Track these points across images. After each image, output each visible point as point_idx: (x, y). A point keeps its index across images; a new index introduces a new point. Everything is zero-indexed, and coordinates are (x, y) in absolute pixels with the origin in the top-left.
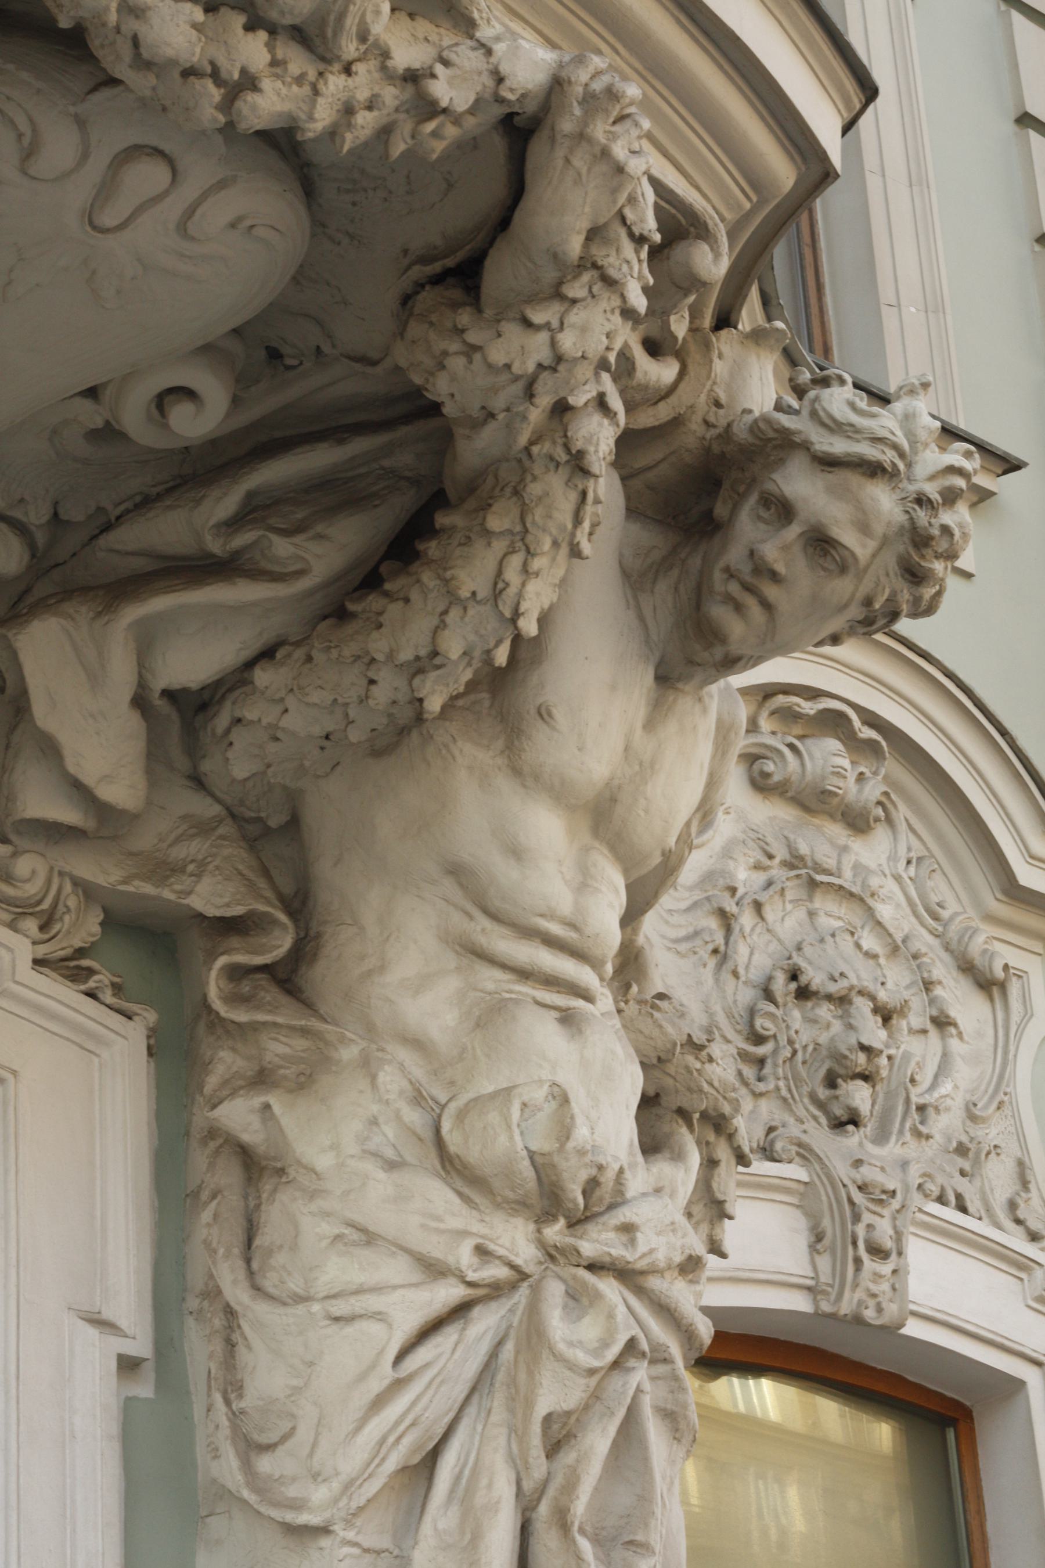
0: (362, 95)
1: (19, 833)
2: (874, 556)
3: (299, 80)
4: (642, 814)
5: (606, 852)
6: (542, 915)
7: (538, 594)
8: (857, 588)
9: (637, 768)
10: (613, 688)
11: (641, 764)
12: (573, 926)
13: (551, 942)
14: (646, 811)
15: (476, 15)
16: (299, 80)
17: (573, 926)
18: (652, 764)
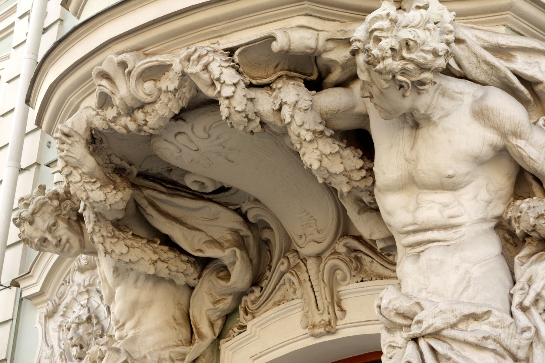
0: (166, 101)
1: (392, 251)
2: (370, 75)
3: (153, 111)
4: (423, 175)
5: (427, 191)
6: (404, 227)
7: (309, 158)
8: (377, 87)
9: (414, 163)
10: (391, 147)
11: (414, 161)
12: (415, 224)
13: (415, 232)
14: (424, 173)
15: (168, 63)
16: (153, 111)
17: (415, 224)
18: (417, 158)
